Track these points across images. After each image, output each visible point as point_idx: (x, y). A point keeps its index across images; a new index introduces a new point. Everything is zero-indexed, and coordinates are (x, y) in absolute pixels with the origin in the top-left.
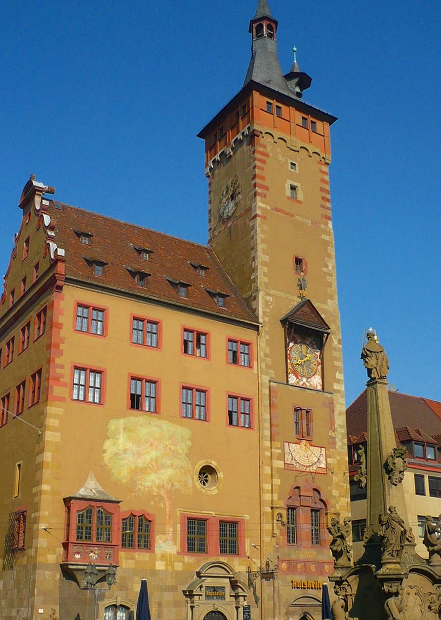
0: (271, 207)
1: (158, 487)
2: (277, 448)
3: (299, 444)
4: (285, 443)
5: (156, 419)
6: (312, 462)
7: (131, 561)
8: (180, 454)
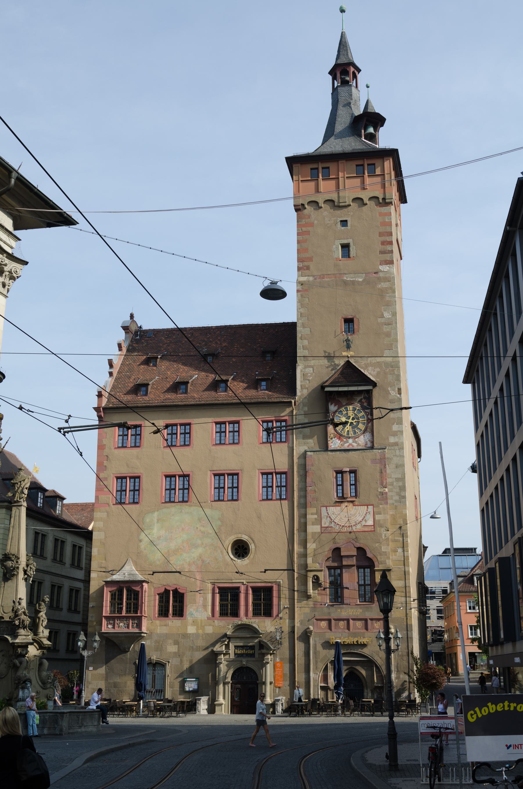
0: (313, 276)
1: (189, 564)
2: (312, 514)
4: (322, 508)
5: (187, 507)
6: (355, 522)
7: (165, 627)
8: (211, 534)
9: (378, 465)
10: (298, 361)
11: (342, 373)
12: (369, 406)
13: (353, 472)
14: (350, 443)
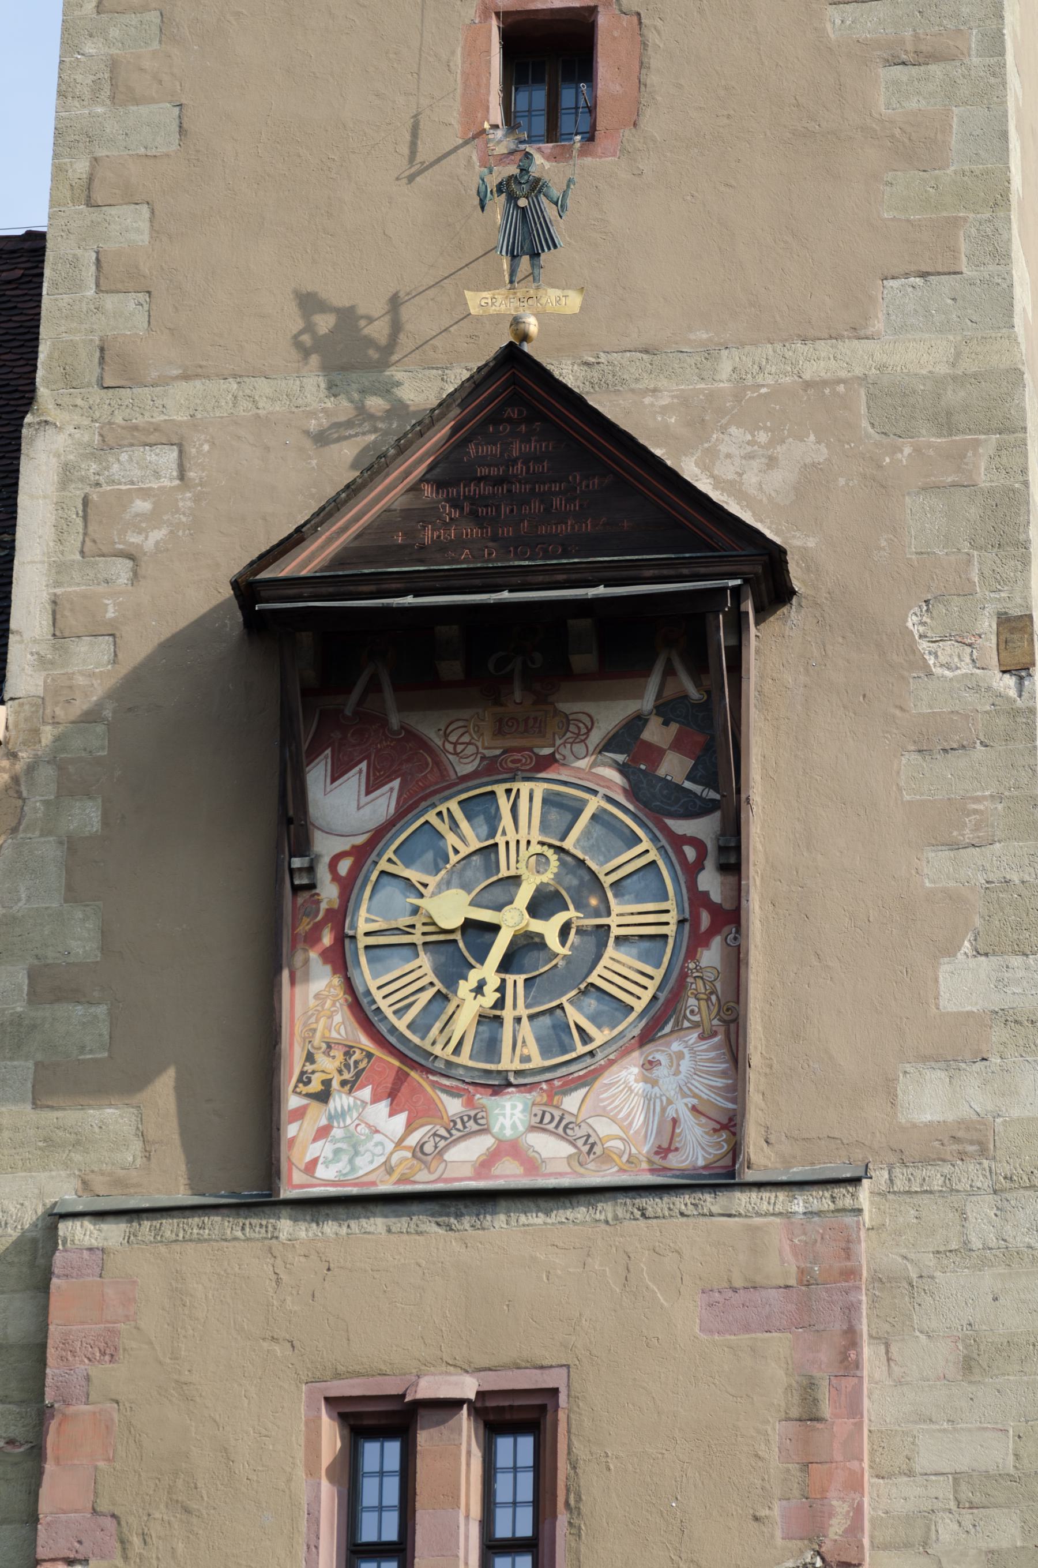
9: (779, 1344)
10: (43, 391)
11: (448, 473)
12: (711, 782)
13: (518, 1415)
14: (509, 1135)
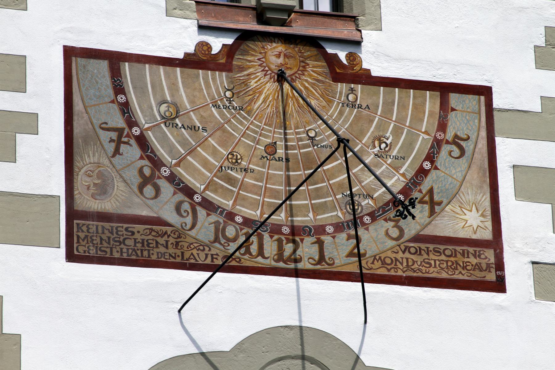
3: (227, 68)
